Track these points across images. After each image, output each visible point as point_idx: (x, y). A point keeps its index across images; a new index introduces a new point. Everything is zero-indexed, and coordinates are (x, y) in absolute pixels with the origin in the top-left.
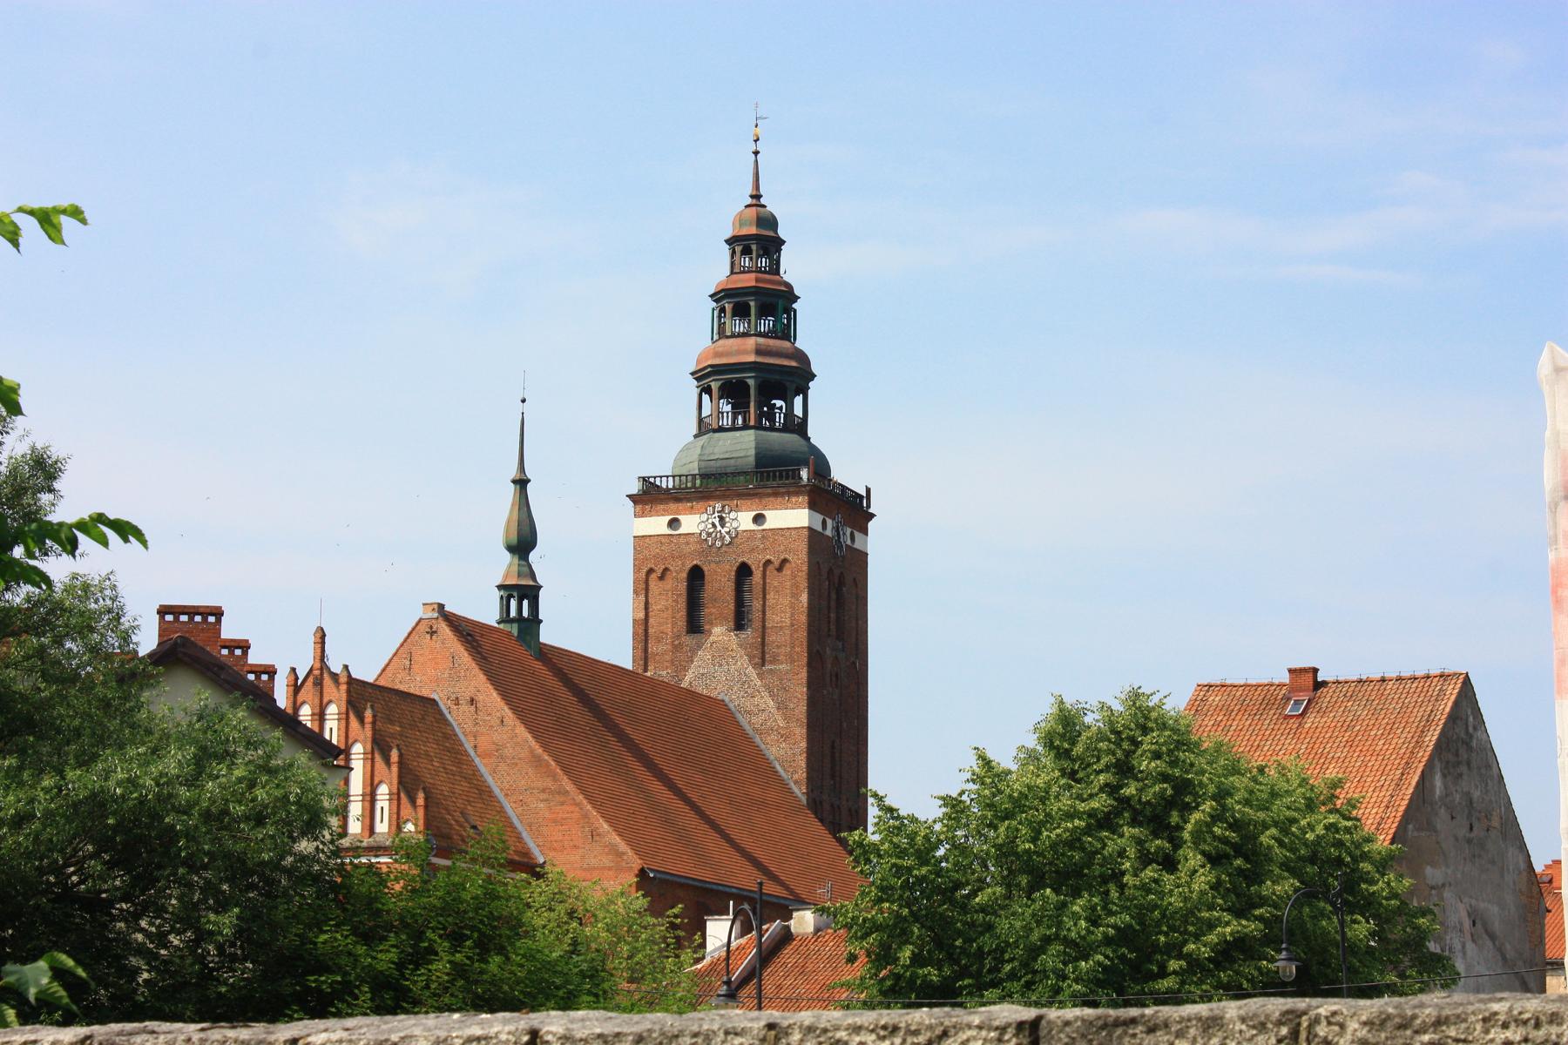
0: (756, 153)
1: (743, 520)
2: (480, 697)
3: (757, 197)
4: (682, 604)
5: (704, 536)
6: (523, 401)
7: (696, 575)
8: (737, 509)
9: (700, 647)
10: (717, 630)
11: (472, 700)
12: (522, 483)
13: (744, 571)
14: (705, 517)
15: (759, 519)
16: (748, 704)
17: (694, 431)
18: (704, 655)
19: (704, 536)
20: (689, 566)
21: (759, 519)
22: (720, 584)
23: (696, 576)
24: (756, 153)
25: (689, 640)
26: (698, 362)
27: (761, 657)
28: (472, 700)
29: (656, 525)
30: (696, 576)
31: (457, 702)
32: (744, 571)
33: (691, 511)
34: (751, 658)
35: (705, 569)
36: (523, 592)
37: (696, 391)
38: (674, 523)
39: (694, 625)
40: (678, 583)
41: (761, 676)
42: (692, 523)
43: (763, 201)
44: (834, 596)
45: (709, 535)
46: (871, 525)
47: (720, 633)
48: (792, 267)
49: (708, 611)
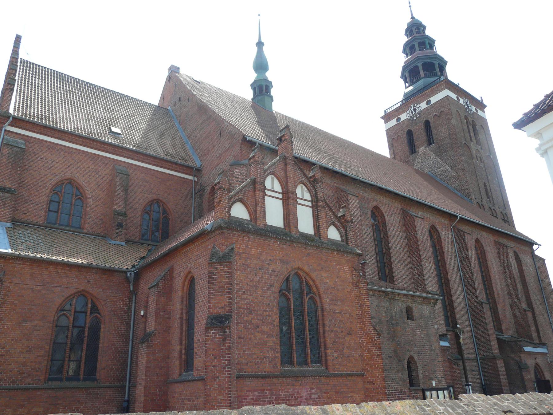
0: (410, 6)
1: (423, 105)
5: (409, 118)
6: (259, 15)
8: (419, 103)
9: (416, 158)
12: (260, 44)
14: (408, 112)
15: (428, 102)
18: (418, 160)
19: (409, 118)
20: (406, 131)
24: (410, 6)
25: (411, 157)
27: (440, 153)
29: (393, 122)
30: (410, 133)
32: (427, 124)
34: (436, 154)
35: (412, 129)
36: (262, 89)
39: (413, 149)
40: (404, 138)
41: (441, 159)
42: (404, 117)
44: (471, 128)
45: (411, 117)
46: (485, 110)
47: (422, 150)
49: (417, 143)
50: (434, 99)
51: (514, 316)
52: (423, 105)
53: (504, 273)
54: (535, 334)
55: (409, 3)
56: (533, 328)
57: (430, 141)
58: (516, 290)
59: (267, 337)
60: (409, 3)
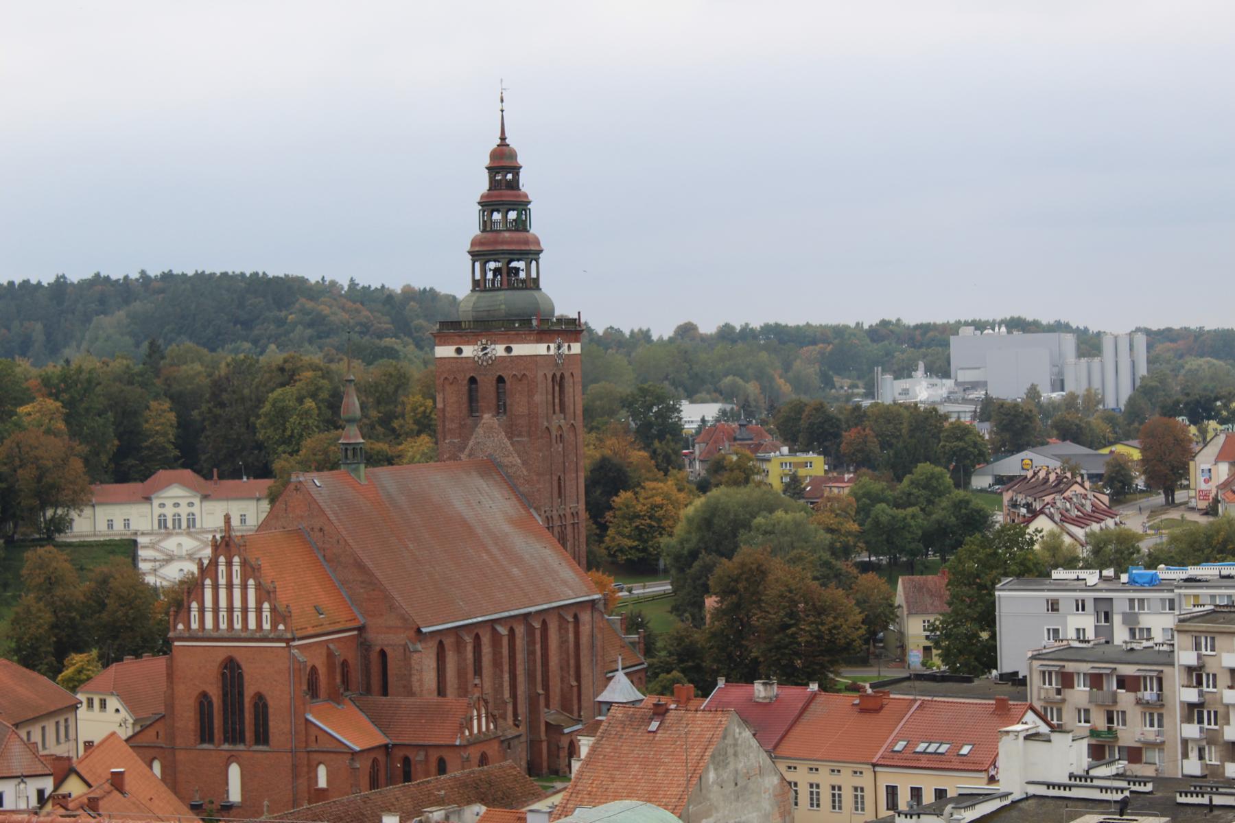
1: (500, 350)
2: (326, 528)
3: (503, 138)
4: (465, 399)
7: (473, 380)
8: (495, 342)
10: (486, 416)
11: (321, 530)
13: (500, 380)
15: (509, 349)
16: (505, 461)
17: (470, 287)
21: (509, 349)
22: (487, 386)
23: (473, 380)
25: (469, 421)
26: (473, 244)
27: (511, 432)
28: (321, 530)
31: (312, 529)
32: (500, 380)
33: (468, 343)
34: (507, 433)
37: (470, 263)
38: (459, 351)
41: (512, 444)
43: (508, 141)
44: (557, 388)
48: (527, 182)
50: (520, 349)
51: (562, 690)
52: (500, 350)
53: (561, 647)
54: (576, 708)
55: (502, 101)
56: (575, 701)
57: (501, 408)
58: (568, 665)
59: (17, 613)
60: (502, 101)
